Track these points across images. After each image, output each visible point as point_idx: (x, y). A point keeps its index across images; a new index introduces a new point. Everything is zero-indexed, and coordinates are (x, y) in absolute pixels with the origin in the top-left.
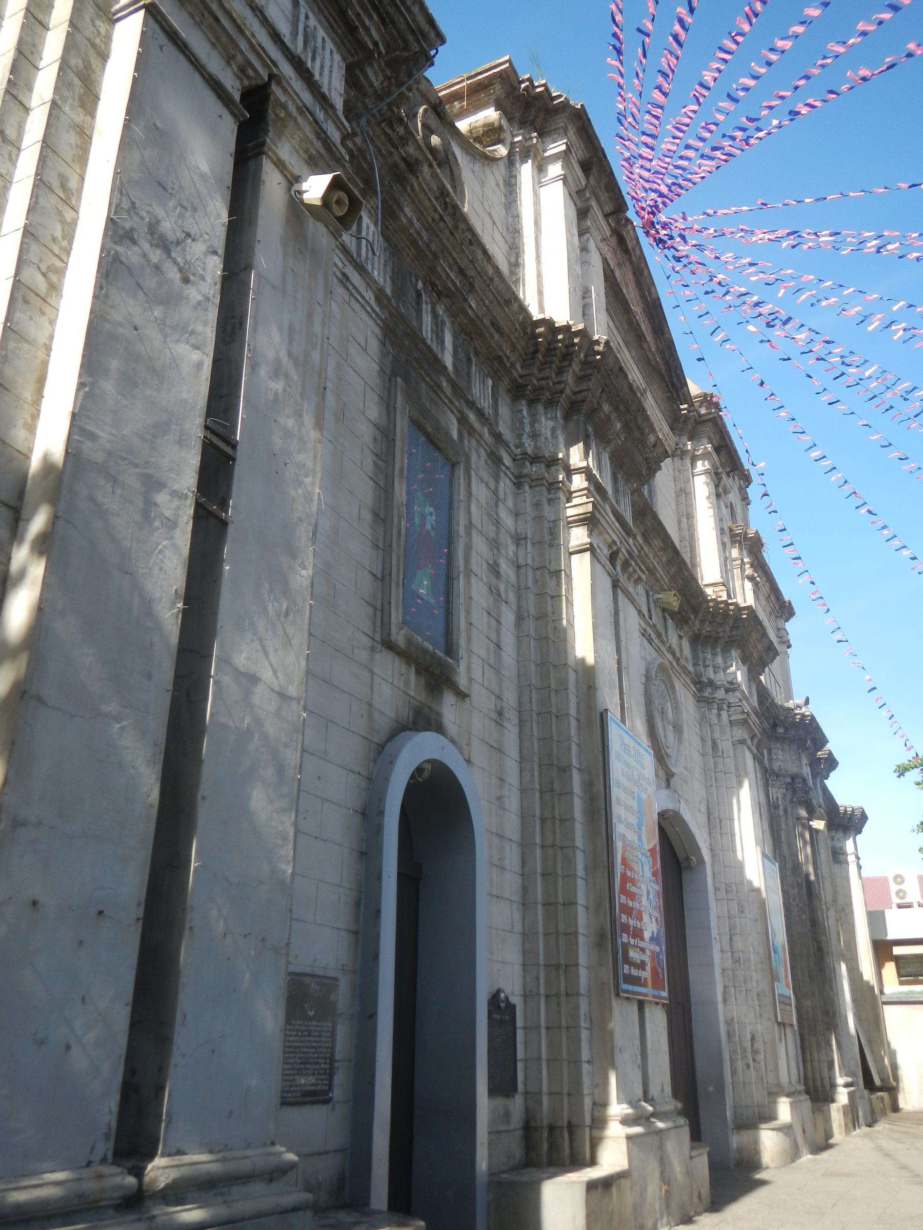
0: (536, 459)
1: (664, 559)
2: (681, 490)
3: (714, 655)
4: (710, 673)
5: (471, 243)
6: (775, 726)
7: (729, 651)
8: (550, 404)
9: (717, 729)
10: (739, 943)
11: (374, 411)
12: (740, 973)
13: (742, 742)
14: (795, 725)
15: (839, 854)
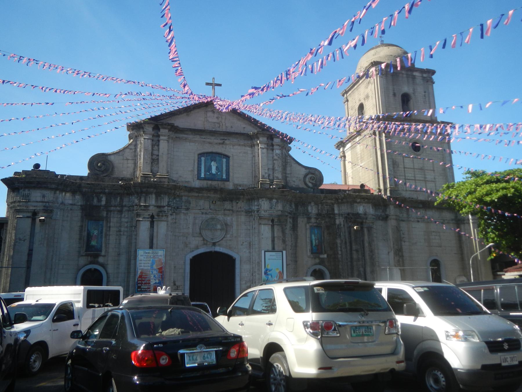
0: (131, 206)
1: (212, 193)
2: (254, 156)
3: (255, 202)
4: (253, 208)
5: (99, 185)
6: (338, 200)
7: (259, 200)
8: (134, 194)
9: (253, 222)
10: (254, 274)
11: (79, 224)
12: (254, 281)
13: (260, 224)
14: (344, 198)
15: (464, 220)
